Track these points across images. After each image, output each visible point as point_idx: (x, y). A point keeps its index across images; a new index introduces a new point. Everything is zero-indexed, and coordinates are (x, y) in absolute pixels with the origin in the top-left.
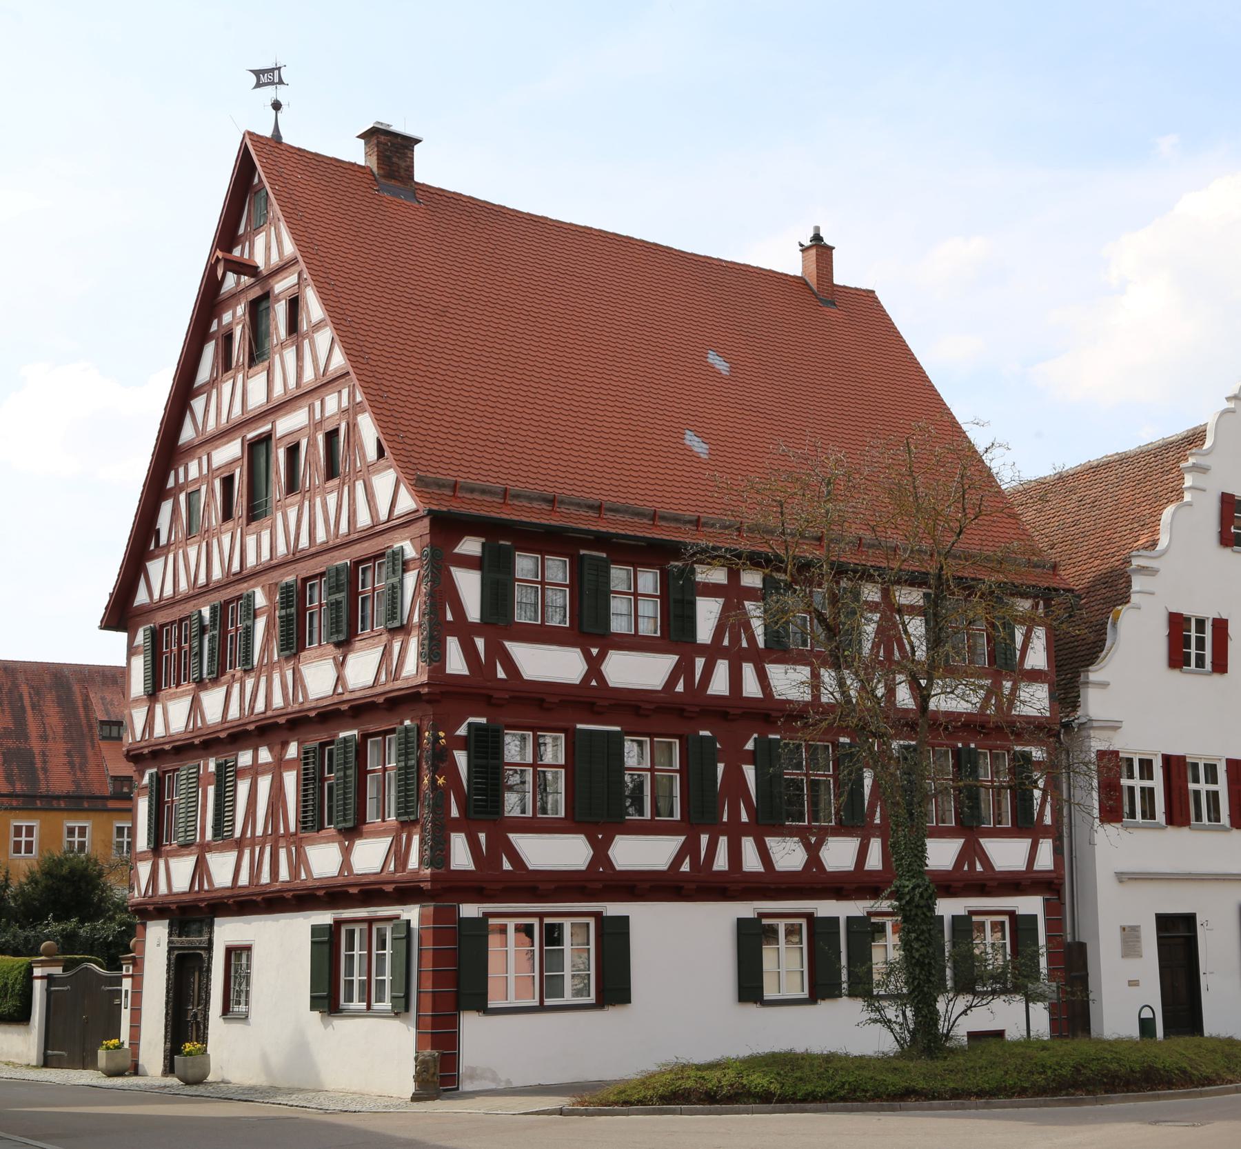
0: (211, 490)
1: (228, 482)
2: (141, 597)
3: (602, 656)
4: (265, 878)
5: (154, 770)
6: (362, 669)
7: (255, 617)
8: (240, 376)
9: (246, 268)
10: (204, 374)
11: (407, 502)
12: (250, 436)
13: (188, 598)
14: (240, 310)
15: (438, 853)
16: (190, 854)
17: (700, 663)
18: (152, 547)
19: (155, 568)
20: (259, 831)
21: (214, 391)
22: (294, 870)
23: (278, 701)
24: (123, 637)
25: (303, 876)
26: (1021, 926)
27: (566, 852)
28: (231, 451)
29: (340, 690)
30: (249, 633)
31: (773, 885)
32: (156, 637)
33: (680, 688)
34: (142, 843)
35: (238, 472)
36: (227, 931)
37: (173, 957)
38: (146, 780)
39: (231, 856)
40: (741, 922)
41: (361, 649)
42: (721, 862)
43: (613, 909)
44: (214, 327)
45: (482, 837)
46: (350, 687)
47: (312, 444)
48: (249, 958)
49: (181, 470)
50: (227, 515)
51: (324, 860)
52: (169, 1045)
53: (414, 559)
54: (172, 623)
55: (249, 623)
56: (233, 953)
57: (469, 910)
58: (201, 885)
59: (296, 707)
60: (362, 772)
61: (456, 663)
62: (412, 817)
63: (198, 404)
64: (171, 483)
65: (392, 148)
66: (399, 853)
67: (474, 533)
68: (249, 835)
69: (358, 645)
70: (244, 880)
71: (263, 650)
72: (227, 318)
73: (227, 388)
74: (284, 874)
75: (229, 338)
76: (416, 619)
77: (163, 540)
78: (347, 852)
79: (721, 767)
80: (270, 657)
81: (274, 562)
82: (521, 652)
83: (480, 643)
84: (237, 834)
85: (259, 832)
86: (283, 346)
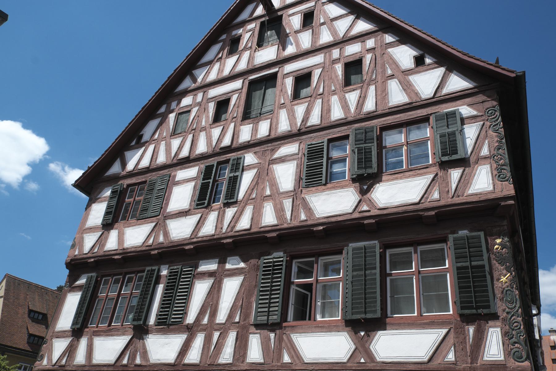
1: (222, 105)
2: (116, 168)
6: (396, 193)
16: (124, 335)
18: (133, 143)
20: (222, 317)
25: (286, 359)
29: (365, 208)
41: (388, 180)
44: (224, 37)
46: (381, 206)
53: (473, 118)
59: (295, 223)
60: (384, 275)
62: (485, 311)
64: (163, 109)
68: (205, 321)
69: (384, 178)
71: (251, 189)
75: (236, 41)
76: (485, 151)
77: (145, 139)
81: (273, 136)
84: (190, 319)
85: (222, 317)
86: (297, 32)
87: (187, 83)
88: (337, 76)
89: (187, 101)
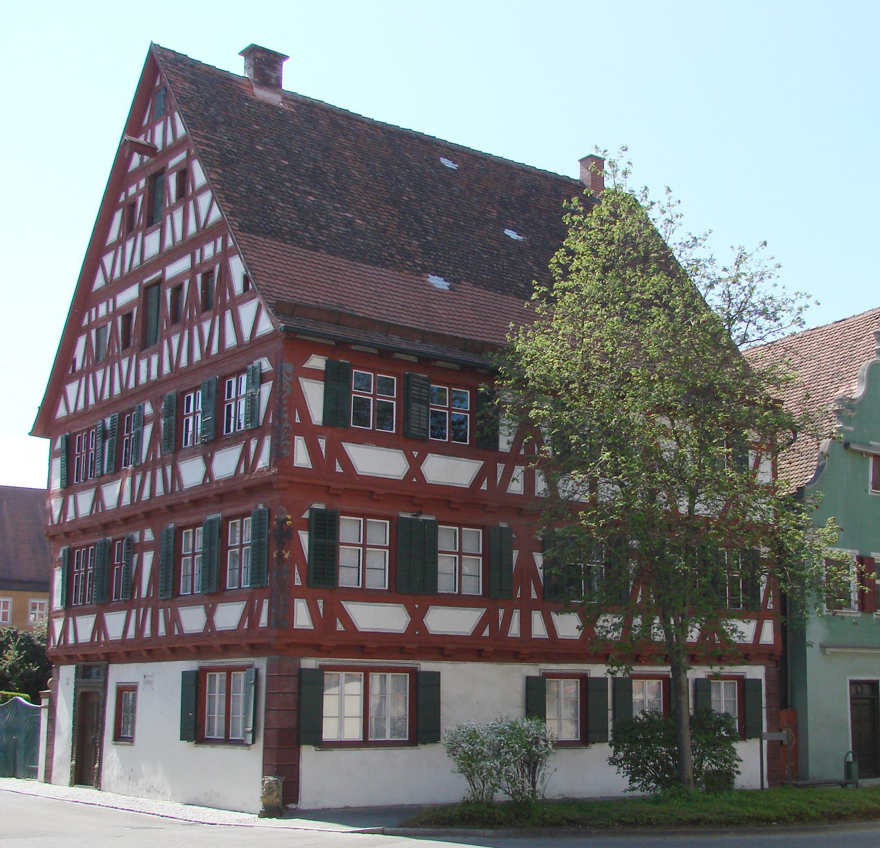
0: (114, 325)
1: (128, 318)
2: (61, 412)
3: (422, 459)
4: (147, 632)
5: (65, 547)
7: (144, 425)
8: (140, 235)
9: (148, 149)
10: (113, 235)
11: (266, 326)
12: (145, 281)
13: (94, 412)
14: (142, 183)
15: (283, 615)
17: (501, 467)
19: (72, 389)
21: (120, 247)
22: (169, 627)
23: (160, 490)
24: (47, 442)
26: (745, 687)
27: (389, 619)
28: (131, 294)
30: (139, 436)
31: (553, 649)
32: (69, 443)
33: (484, 487)
34: (57, 604)
35: (135, 309)
36: (119, 674)
37: (78, 694)
38: (61, 554)
39: (121, 616)
40: (529, 679)
42: (514, 630)
43: (426, 666)
44: (122, 198)
45: (320, 603)
47: (193, 283)
48: (135, 697)
49: (94, 310)
50: (126, 344)
51: (192, 620)
52: (74, 762)
54: (83, 431)
55: (140, 429)
56: (122, 690)
57: (309, 663)
58: (99, 638)
61: (302, 457)
63: (108, 260)
64: (86, 322)
65: (265, 62)
66: (251, 614)
67: (319, 350)
70: (131, 633)
72: (132, 190)
73: (129, 245)
74: (162, 630)
75: (133, 206)
78: (210, 614)
79: (515, 554)
80: (155, 456)
82: (353, 451)
83: (322, 443)
87: (99, 282)
88: (198, 297)
89: (103, 309)
